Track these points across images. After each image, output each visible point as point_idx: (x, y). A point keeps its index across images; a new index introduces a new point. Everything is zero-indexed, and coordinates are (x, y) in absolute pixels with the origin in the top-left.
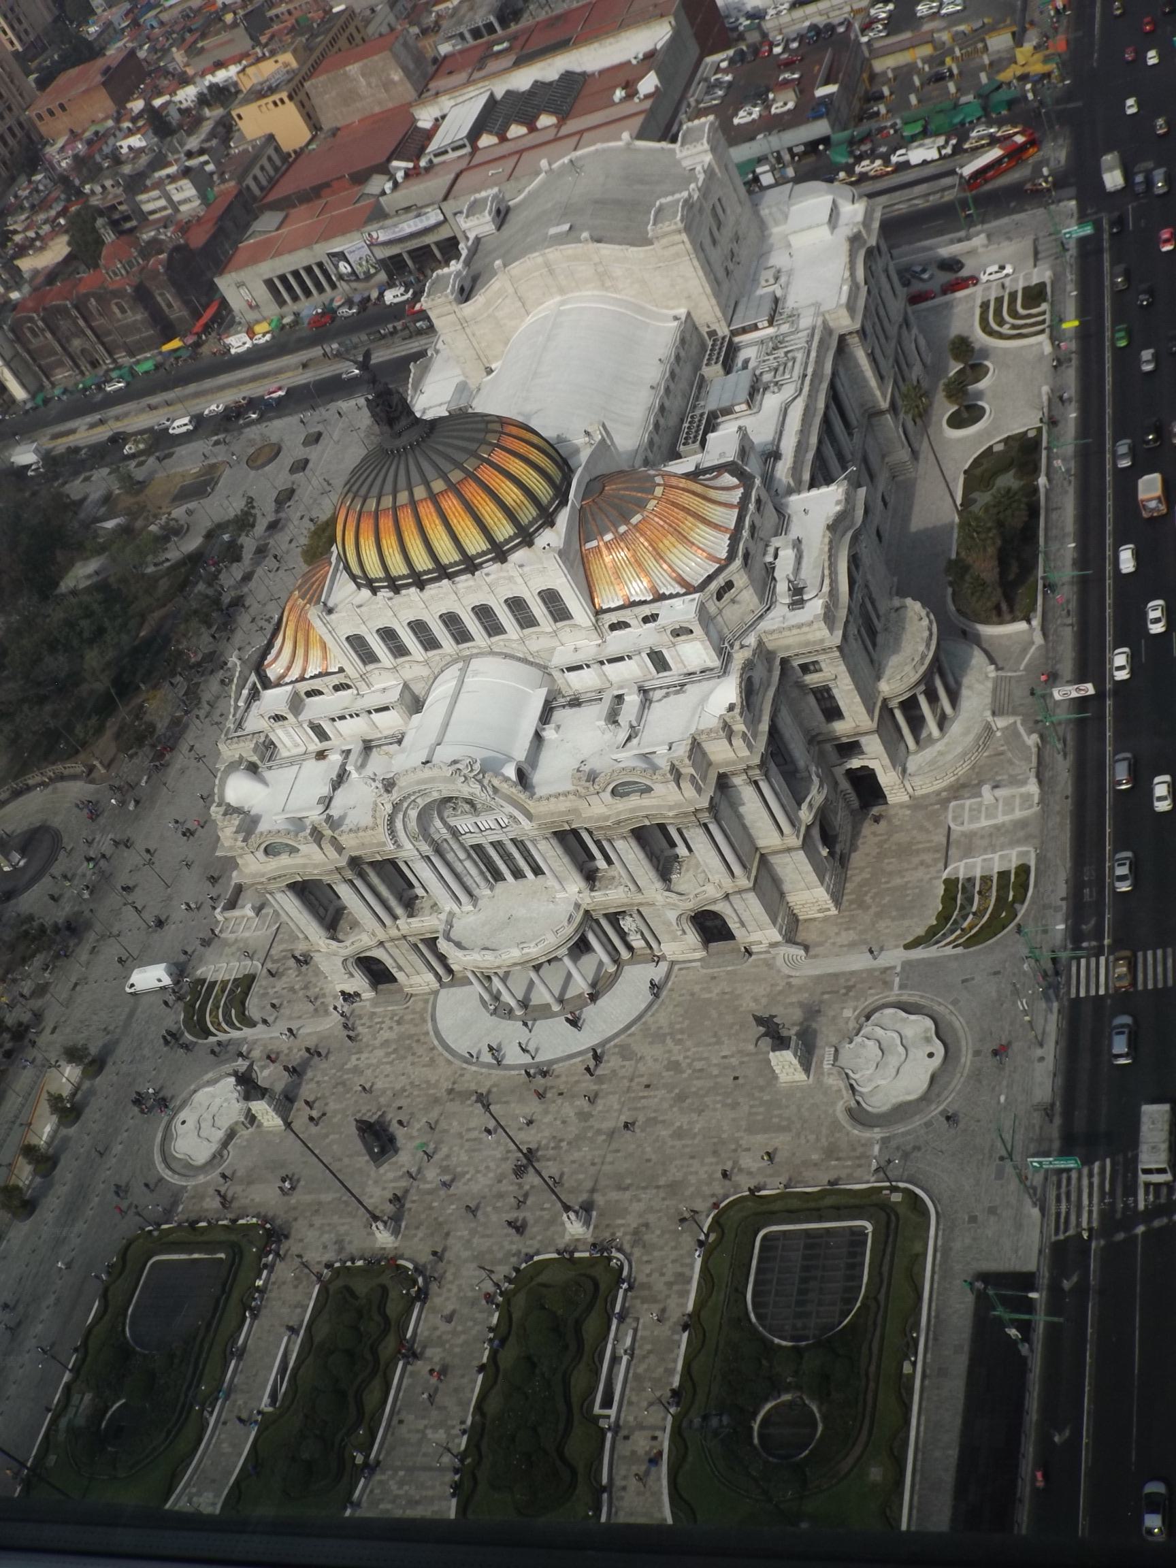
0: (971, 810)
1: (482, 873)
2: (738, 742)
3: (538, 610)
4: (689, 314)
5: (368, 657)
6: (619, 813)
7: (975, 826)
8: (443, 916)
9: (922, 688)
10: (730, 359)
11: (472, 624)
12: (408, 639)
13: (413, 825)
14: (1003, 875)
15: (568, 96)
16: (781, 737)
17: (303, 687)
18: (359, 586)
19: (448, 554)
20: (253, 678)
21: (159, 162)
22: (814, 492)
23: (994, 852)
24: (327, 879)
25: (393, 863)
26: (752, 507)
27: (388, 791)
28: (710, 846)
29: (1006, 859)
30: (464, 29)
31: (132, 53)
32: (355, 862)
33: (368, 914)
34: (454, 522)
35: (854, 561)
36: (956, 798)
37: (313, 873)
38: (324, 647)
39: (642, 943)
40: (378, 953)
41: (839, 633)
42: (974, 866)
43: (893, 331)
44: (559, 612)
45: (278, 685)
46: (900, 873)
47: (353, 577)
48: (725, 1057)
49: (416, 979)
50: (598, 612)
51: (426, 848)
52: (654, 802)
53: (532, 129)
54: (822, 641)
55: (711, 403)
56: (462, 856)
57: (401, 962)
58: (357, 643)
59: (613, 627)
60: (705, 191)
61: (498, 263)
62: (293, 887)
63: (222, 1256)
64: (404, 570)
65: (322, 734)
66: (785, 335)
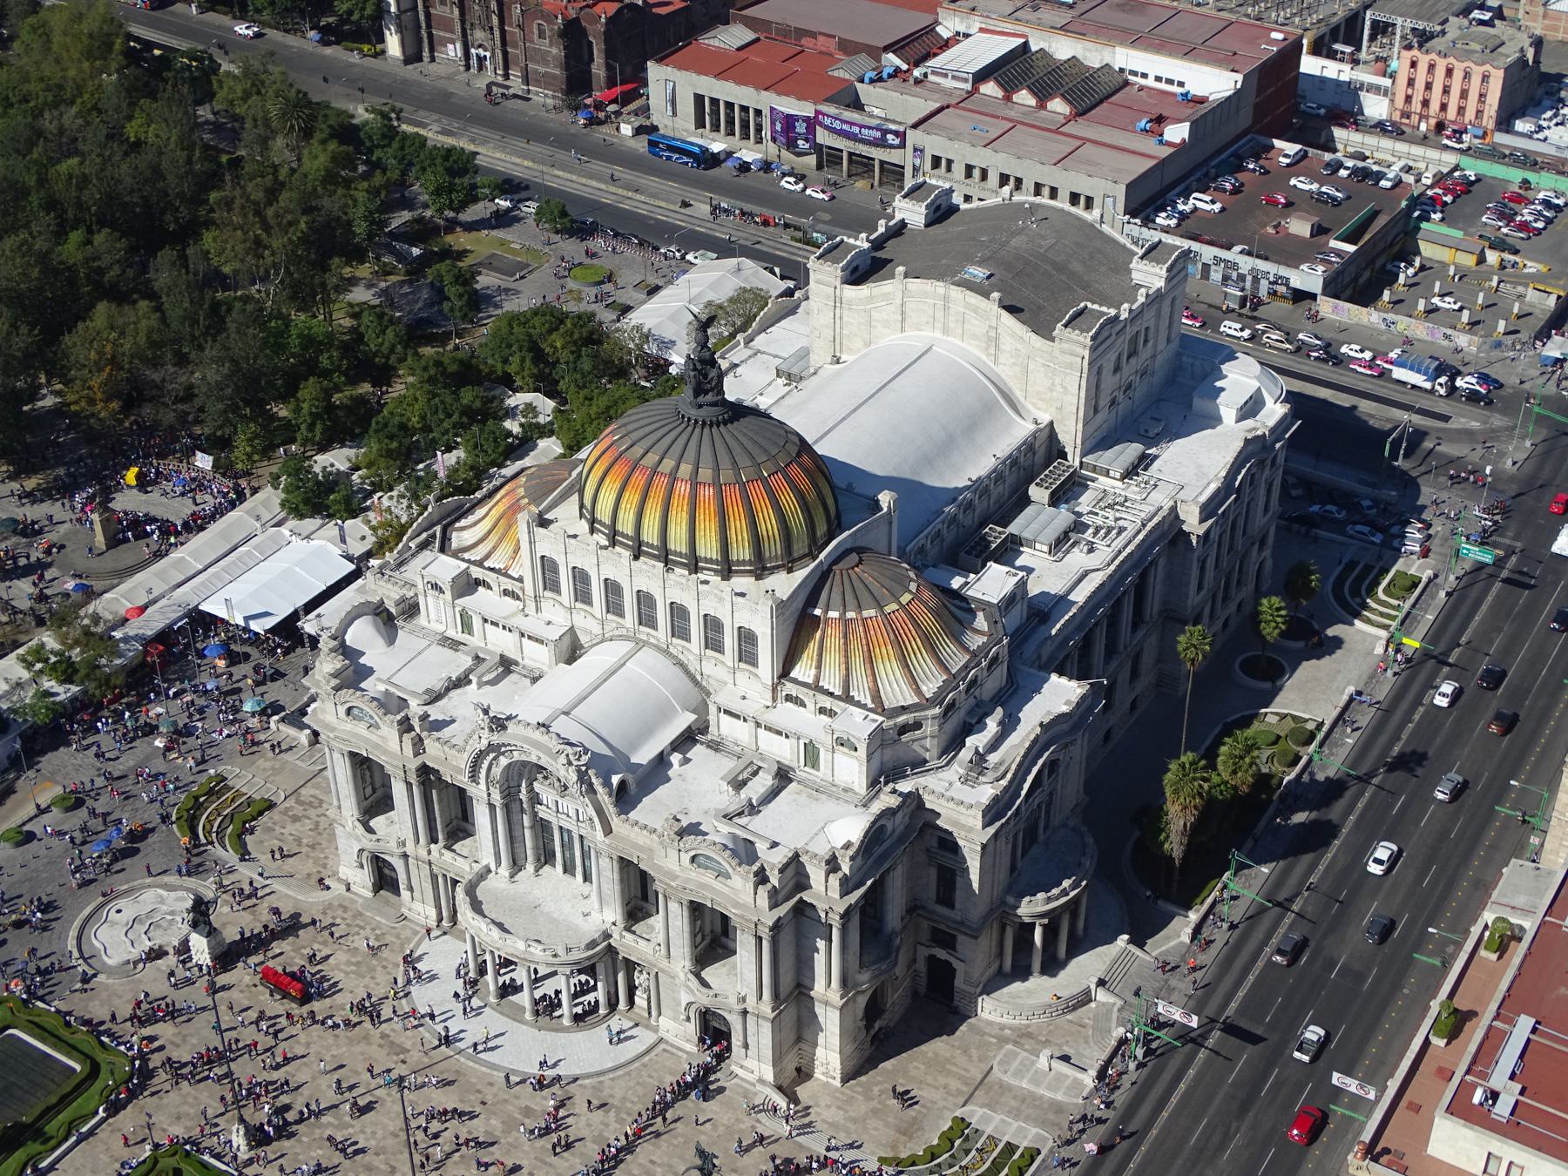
0: (1021, 1063)
1: (536, 848)
2: (834, 881)
3: (730, 641)
4: (1052, 423)
5: (552, 585)
6: (688, 880)
7: (1014, 1082)
8: (477, 867)
9: (1046, 921)
10: (1065, 493)
13: (497, 771)
14: (1010, 1148)
15: (1092, 93)
16: (883, 893)
17: (476, 572)
18: (581, 516)
19: (678, 540)
20: (438, 529)
23: (1017, 1117)
24: (389, 769)
25: (462, 791)
29: (1025, 1134)
32: (424, 770)
34: (700, 517)
35: (1052, 765)
36: (1016, 1043)
38: (517, 550)
39: (645, 1004)
40: (398, 864)
41: (991, 830)
42: (990, 1120)
43: (1239, 543)
45: (455, 555)
47: (582, 506)
48: (652, 1162)
49: (417, 906)
51: (497, 797)
52: (725, 890)
53: (1042, 105)
54: (971, 829)
58: (548, 568)
59: (789, 698)
60: (1135, 316)
61: (901, 269)
62: (353, 755)
63: (78, 1068)
64: (629, 531)
65: (467, 627)
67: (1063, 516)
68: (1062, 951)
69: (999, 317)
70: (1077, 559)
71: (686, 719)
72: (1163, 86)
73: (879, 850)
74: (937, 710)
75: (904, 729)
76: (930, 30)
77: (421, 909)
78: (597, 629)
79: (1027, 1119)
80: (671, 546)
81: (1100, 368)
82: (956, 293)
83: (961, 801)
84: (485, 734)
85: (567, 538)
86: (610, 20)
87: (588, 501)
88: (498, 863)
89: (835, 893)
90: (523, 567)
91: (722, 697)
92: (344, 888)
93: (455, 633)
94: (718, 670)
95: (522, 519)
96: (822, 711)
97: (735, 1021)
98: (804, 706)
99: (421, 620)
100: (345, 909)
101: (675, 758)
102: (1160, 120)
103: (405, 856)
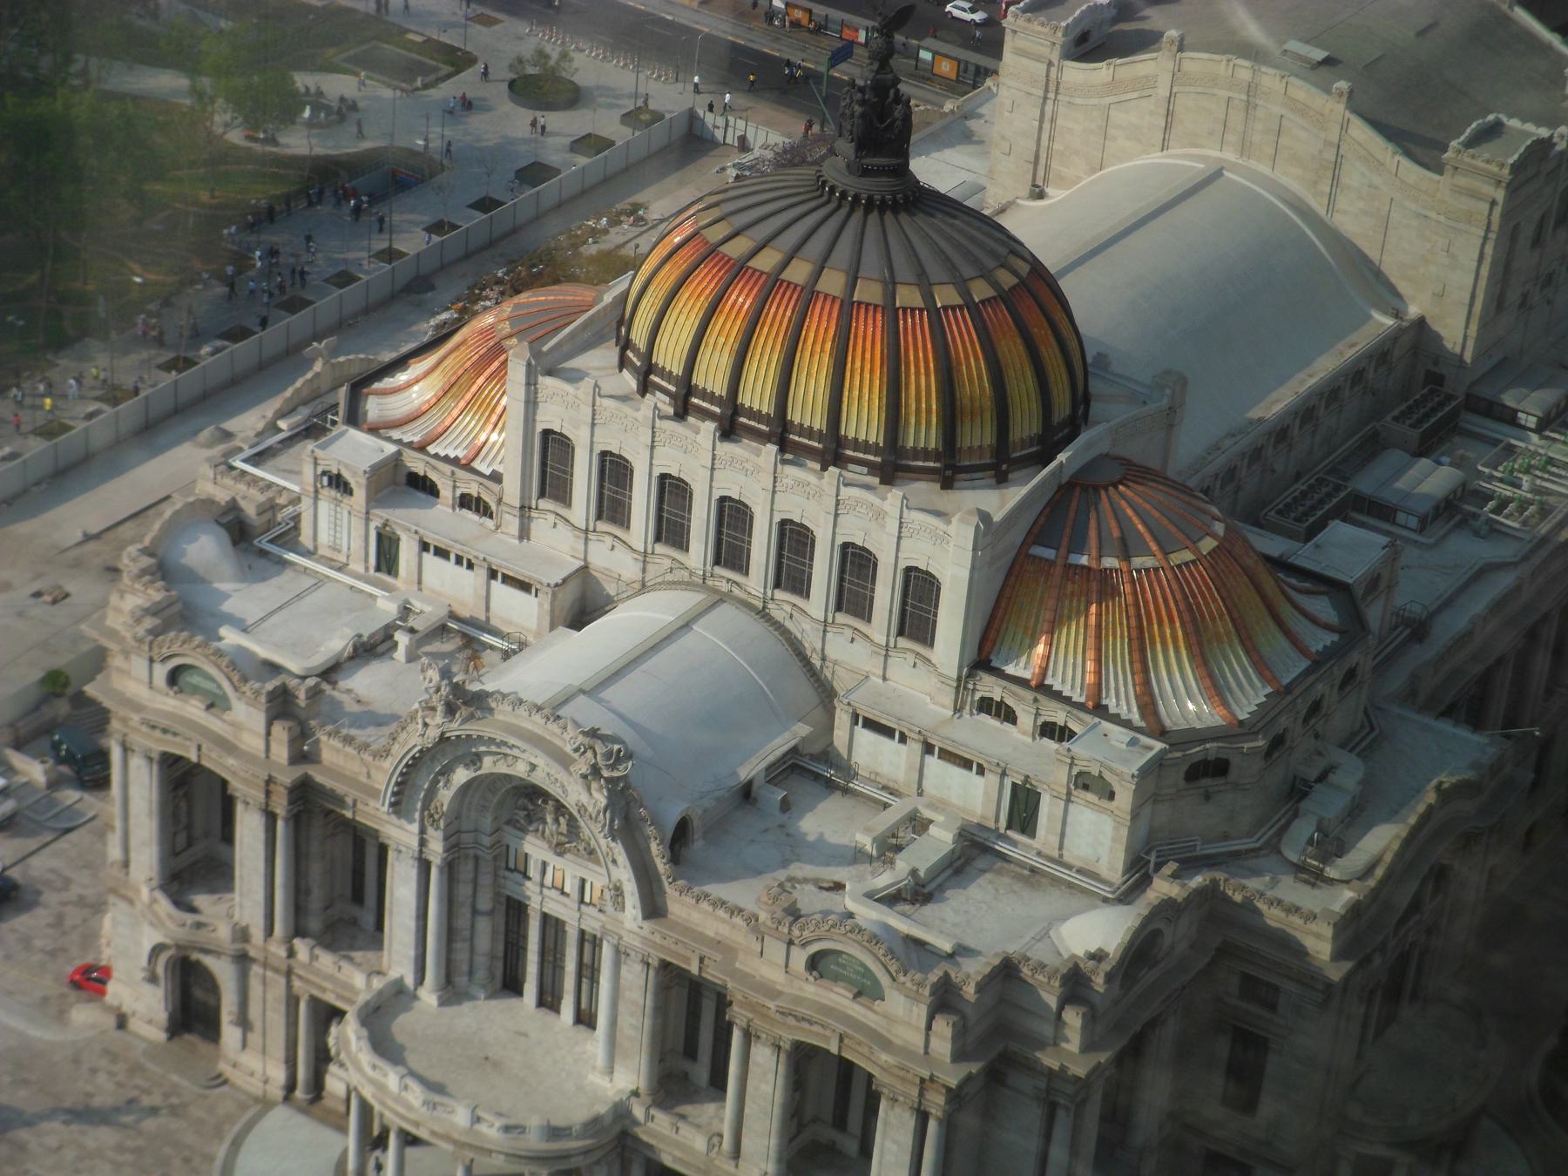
3: (885, 594)
6: (799, 1000)
8: (378, 984)
13: (445, 796)
17: (416, 463)
18: (623, 363)
19: (808, 409)
22: (1446, 726)
24: (237, 787)
26: (1339, 672)
27: (451, 710)
33: (260, 895)
34: (855, 363)
37: (215, 761)
44: (916, 619)
45: (374, 430)
49: (251, 1060)
51: (436, 848)
55: (1365, 483)
56: (484, 903)
57: (254, 1012)
59: (986, 706)
64: (719, 387)
65: (387, 558)
66: (1551, 461)
69: (1344, 127)
73: (1149, 977)
74: (1261, 743)
80: (795, 416)
81: (1516, 227)
88: (420, 980)
92: (111, 1021)
98: (1010, 716)
100: (113, 1057)
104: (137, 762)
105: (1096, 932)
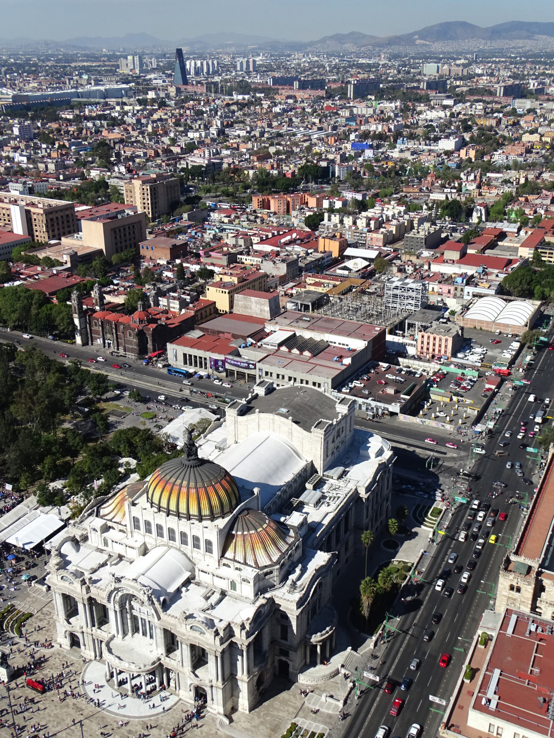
1: (132, 626)
2: (244, 633)
3: (202, 544)
5: (137, 527)
8: (110, 635)
10: (318, 485)
11: (178, 536)
12: (154, 529)
13: (117, 598)
15: (318, 349)
17: (109, 524)
19: (183, 509)
20: (95, 508)
21: (174, 290)
23: (315, 721)
24: (77, 599)
25: (104, 606)
28: (215, 665)
29: (318, 728)
30: (299, 302)
31: (186, 245)
32: (90, 599)
35: (320, 585)
38: (124, 515)
40: (80, 636)
41: (300, 610)
42: (305, 723)
44: (209, 549)
45: (102, 517)
46: (278, 710)
49: (87, 652)
50: (223, 556)
51: (117, 608)
53: (301, 353)
54: (292, 610)
58: (136, 521)
59: (224, 565)
60: (338, 423)
64: (165, 506)
65: (106, 544)
67: (318, 494)
68: (328, 655)
70: (324, 509)
71: (187, 575)
72: (341, 346)
73: (259, 620)
74: (278, 567)
75: (266, 574)
76: (262, 330)
77: (88, 652)
78: (154, 543)
79: (319, 722)
80: (180, 511)
82: (277, 417)
83: (288, 599)
84: (113, 584)
85: (143, 510)
86: (154, 330)
87: (150, 496)
89: (244, 637)
90: (127, 521)
91: (200, 565)
93: (102, 547)
94: (198, 555)
95: (126, 503)
96: (237, 569)
97: (208, 690)
99: (89, 542)
100: (59, 654)
101: (184, 589)
102: (341, 357)
103: (83, 632)
104: (57, 595)
105: (248, 612)
